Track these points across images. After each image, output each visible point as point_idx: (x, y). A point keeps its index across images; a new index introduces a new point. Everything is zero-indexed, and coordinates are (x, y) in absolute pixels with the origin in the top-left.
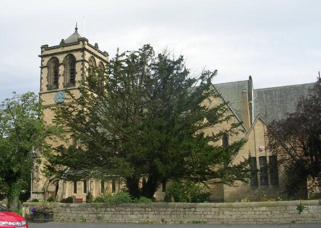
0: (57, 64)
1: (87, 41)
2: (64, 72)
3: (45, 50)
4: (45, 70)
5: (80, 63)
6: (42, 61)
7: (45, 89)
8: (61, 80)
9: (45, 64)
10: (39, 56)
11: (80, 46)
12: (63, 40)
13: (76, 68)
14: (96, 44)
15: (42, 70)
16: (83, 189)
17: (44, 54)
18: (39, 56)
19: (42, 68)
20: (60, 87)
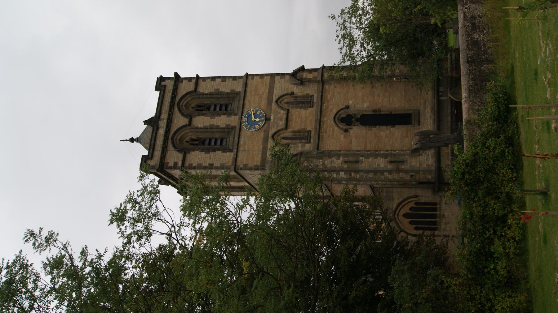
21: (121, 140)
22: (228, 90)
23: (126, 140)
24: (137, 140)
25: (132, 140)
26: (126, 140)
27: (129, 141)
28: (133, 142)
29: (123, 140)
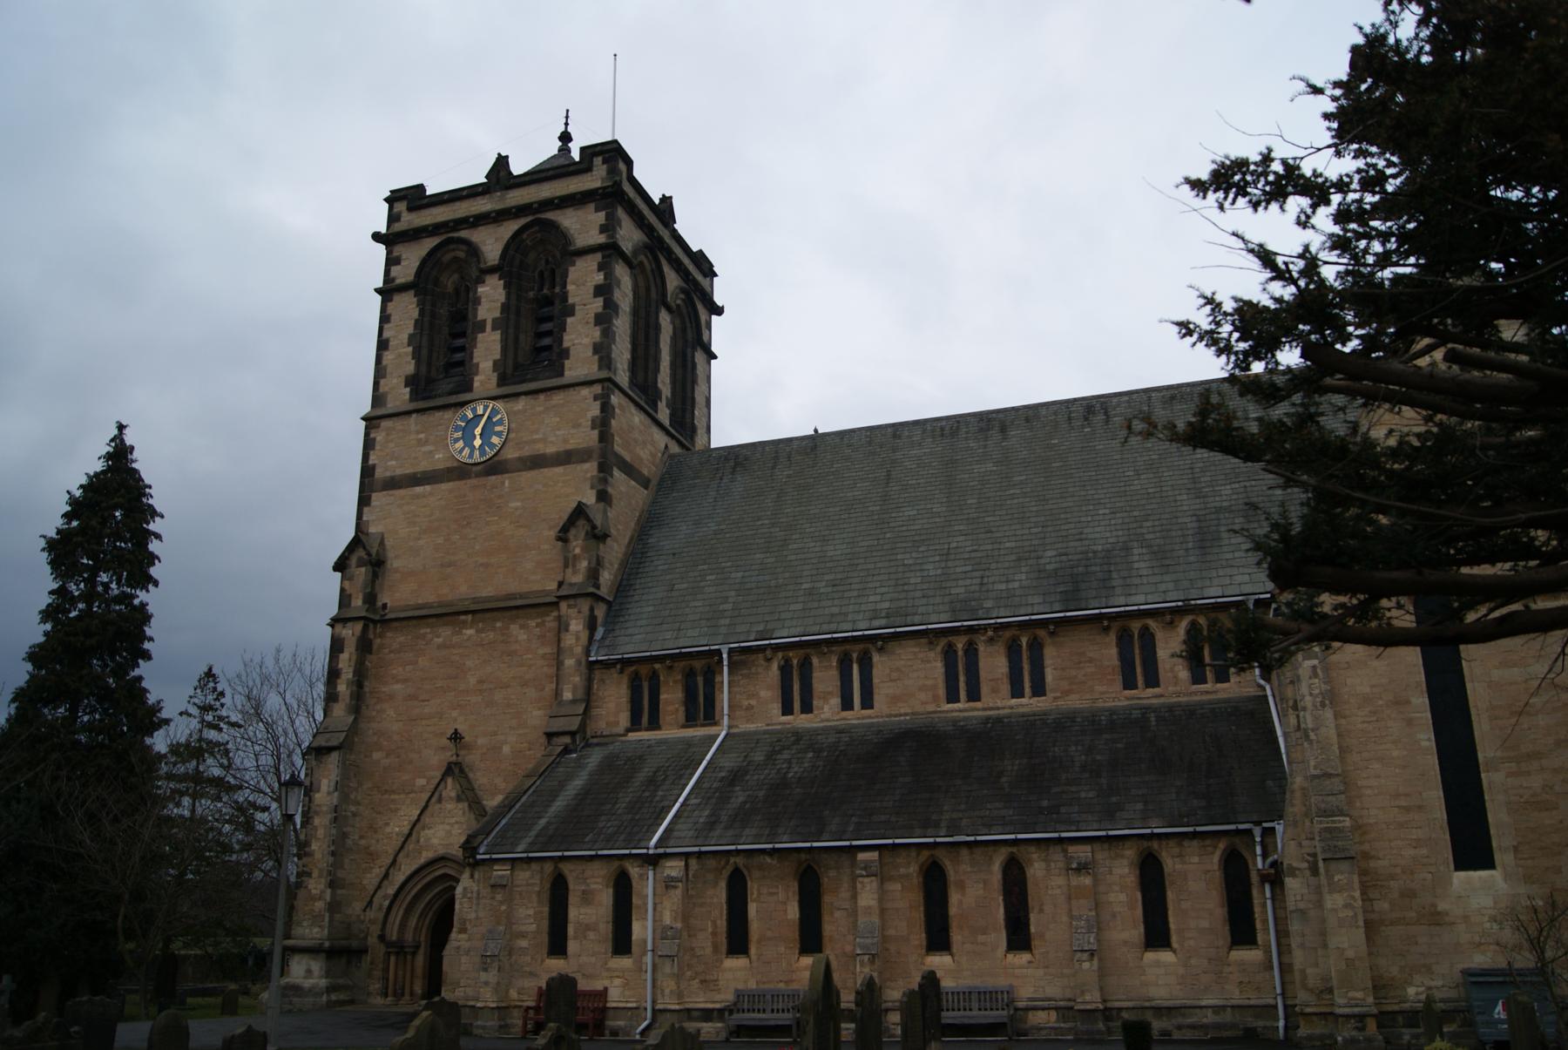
0: (470, 267)
1: (629, 163)
2: (505, 308)
3: (410, 209)
4: (407, 308)
5: (592, 262)
6: (391, 261)
7: (400, 395)
8: (487, 350)
9: (405, 273)
10: (377, 237)
11: (595, 179)
12: (502, 162)
13: (570, 287)
14: (667, 200)
15: (390, 305)
16: (606, 928)
17: (398, 227)
18: (377, 237)
19: (387, 292)
20: (478, 381)
21: (568, 111)
22: (568, 340)
23: (566, 124)
24: (564, 150)
25: (565, 137)
26: (566, 124)
27: (562, 129)
28: (560, 138)
29: (567, 117)
